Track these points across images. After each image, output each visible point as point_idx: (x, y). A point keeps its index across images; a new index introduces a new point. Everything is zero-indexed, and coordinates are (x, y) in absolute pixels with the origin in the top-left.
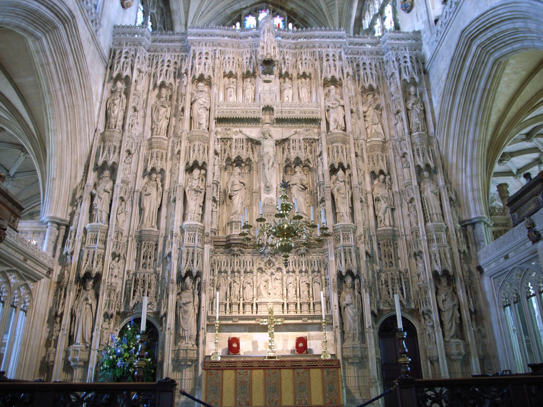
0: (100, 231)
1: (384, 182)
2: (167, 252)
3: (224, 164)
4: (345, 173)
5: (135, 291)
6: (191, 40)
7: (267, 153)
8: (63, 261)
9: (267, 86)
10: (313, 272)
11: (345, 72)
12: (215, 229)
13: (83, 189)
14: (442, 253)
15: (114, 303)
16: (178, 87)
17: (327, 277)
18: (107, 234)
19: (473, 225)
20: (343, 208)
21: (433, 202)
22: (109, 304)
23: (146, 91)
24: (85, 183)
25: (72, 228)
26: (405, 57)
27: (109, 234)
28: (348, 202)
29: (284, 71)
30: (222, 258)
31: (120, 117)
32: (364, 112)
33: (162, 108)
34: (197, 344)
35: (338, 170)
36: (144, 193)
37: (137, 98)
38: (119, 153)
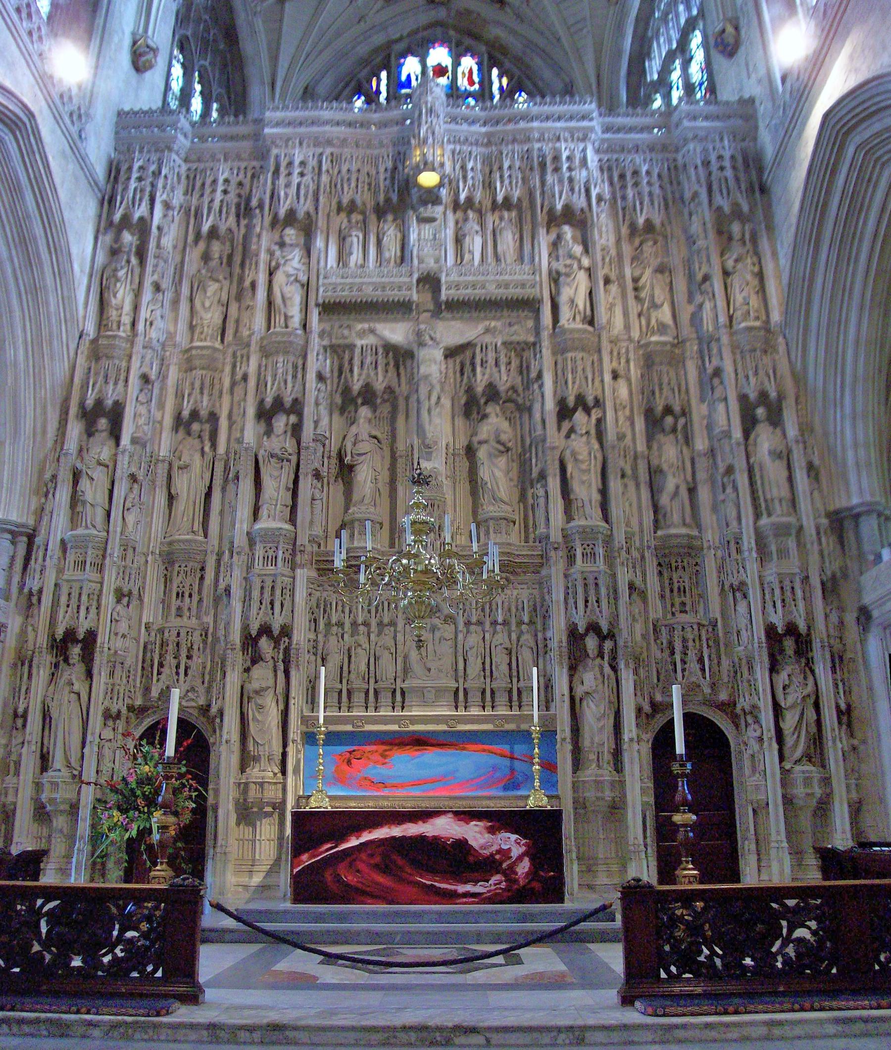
0: (90, 545)
2: (222, 585)
3: (338, 400)
4: (589, 415)
5: (161, 665)
6: (271, 135)
7: (426, 377)
9: (428, 230)
11: (594, 194)
12: (317, 536)
13: (58, 461)
15: (122, 691)
16: (246, 237)
17: (549, 634)
18: (105, 549)
21: (774, 471)
22: (111, 692)
23: (180, 246)
25: (39, 540)
26: (720, 158)
27: (109, 551)
29: (463, 196)
31: (127, 307)
32: (636, 280)
33: (211, 283)
34: (284, 772)
35: (574, 410)
37: (161, 263)
38: (126, 381)
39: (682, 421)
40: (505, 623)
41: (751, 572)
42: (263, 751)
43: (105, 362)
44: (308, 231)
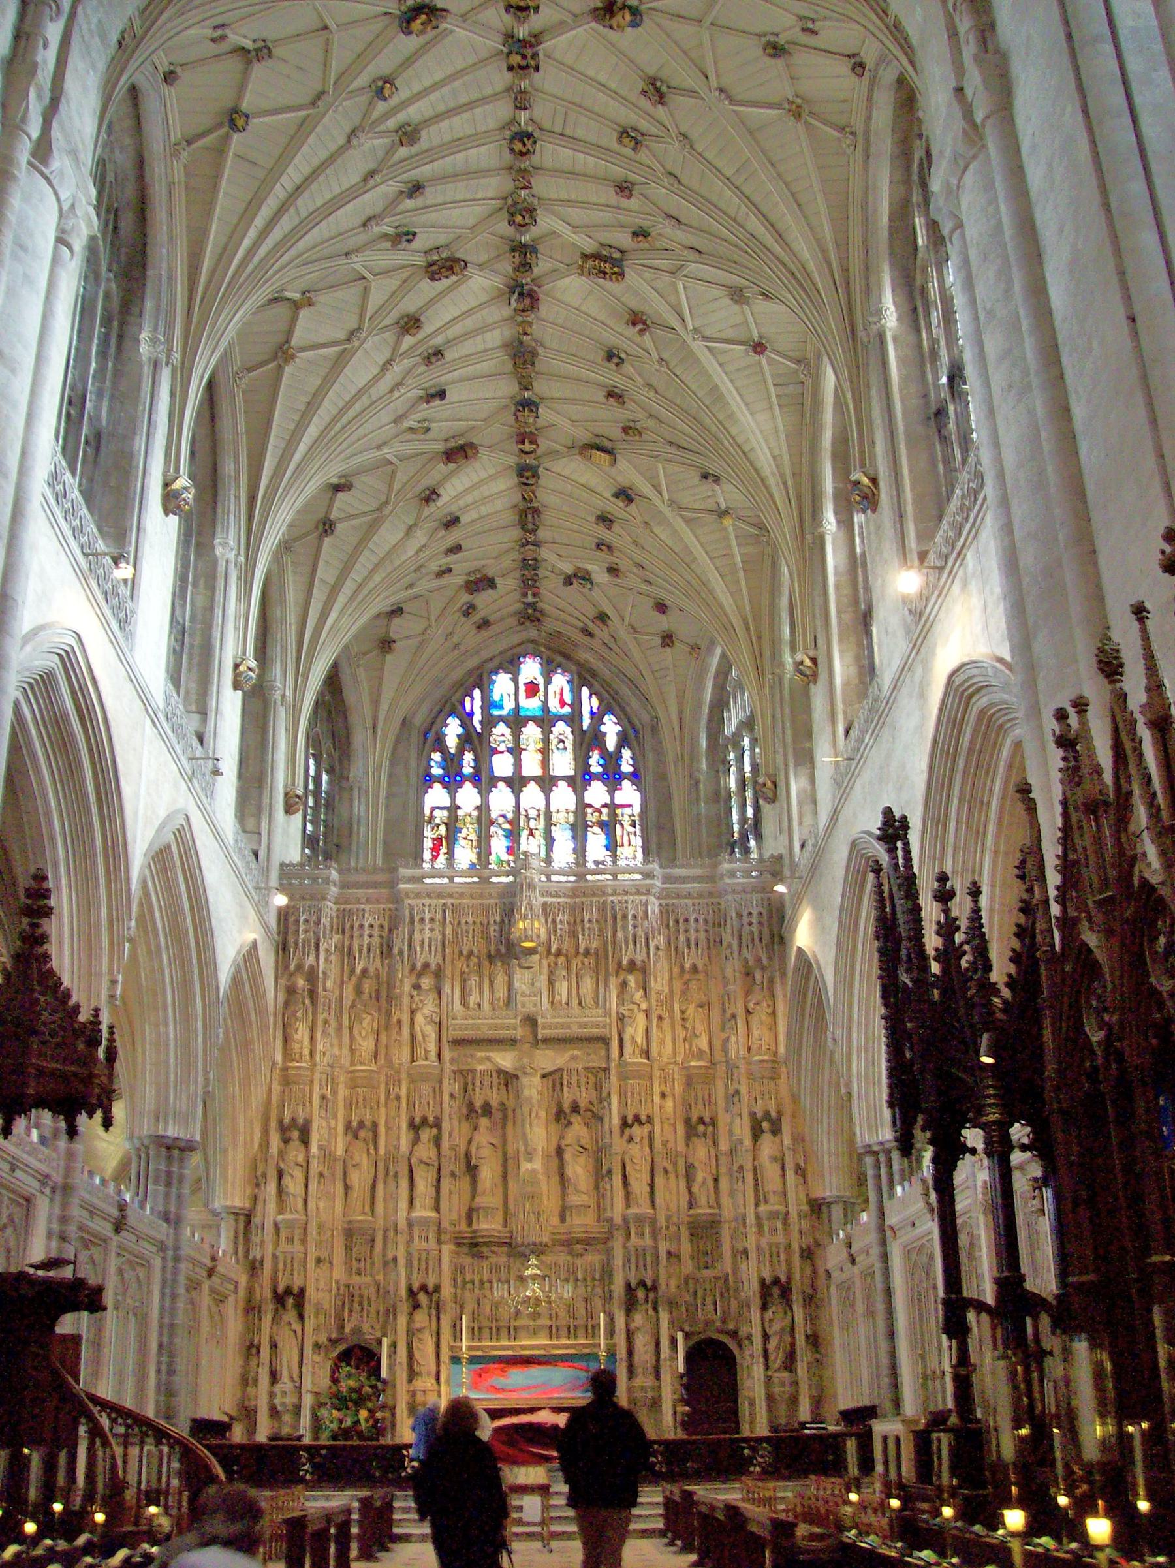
2: (390, 1255)
3: (465, 1111)
16: (388, 974)
19: (829, 1204)
20: (639, 1186)
21: (771, 1171)
22: (316, 1330)
28: (646, 1177)
30: (467, 1261)
32: (683, 1012)
36: (350, 1163)
40: (585, 1280)
41: (751, 1244)
42: (424, 1370)
43: (294, 1087)
44: (438, 974)
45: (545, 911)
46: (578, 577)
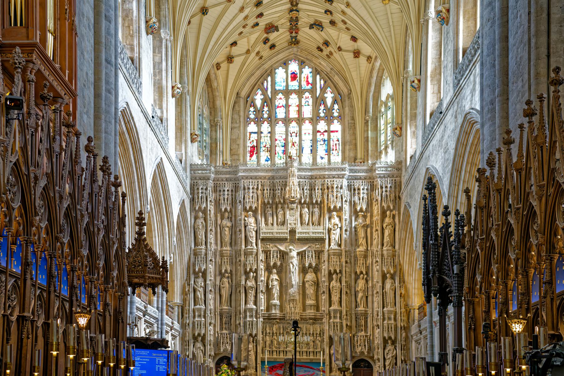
1: (363, 278)
2: (238, 322)
8: (183, 326)
10: (317, 334)
11: (344, 200)
14: (390, 327)
20: (335, 298)
24: (190, 282)
26: (386, 187)
28: (338, 296)
35: (334, 274)
39: (365, 276)
45: (299, 185)
46: (317, 25)
